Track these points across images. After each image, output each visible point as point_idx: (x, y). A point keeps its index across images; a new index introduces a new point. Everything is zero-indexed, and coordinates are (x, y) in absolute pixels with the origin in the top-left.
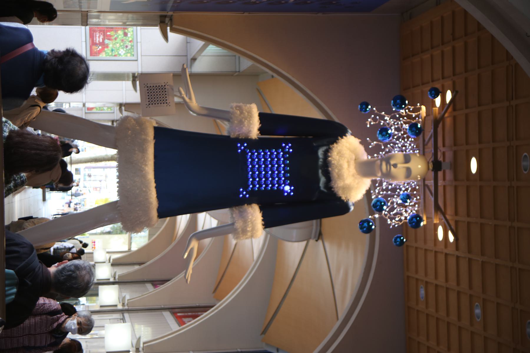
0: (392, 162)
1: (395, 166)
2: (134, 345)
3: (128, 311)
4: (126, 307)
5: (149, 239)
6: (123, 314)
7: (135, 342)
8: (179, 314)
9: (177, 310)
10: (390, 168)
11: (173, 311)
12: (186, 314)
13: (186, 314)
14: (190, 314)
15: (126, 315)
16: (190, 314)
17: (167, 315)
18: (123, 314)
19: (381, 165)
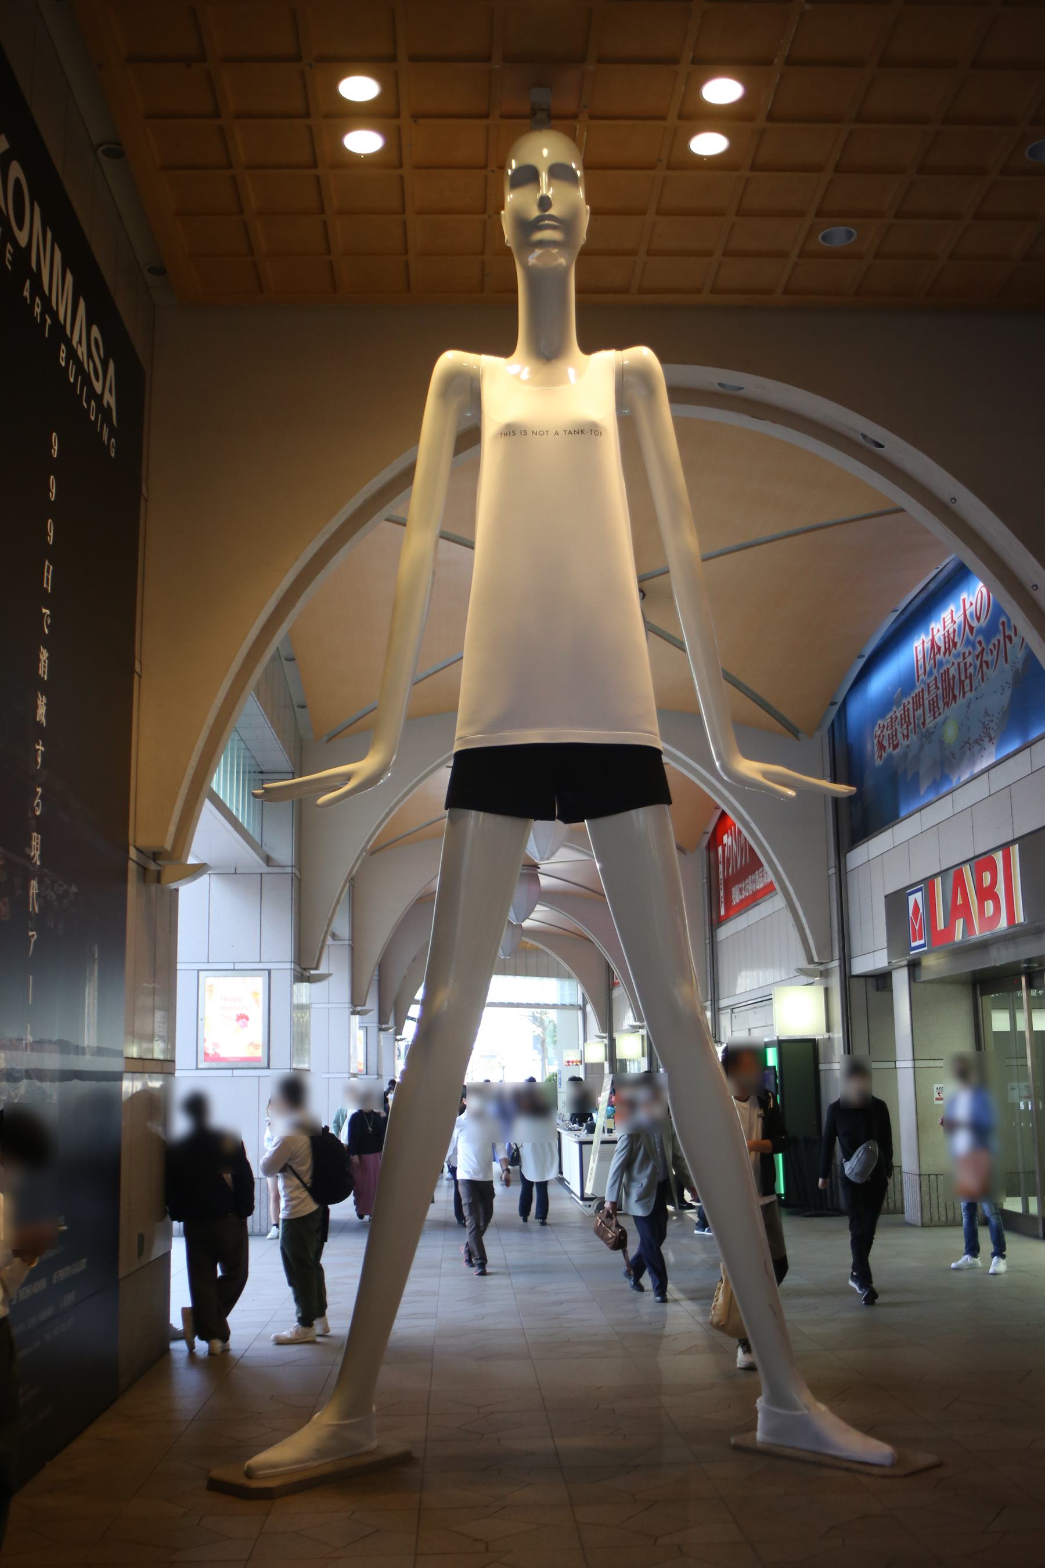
0: (535, 212)
1: (544, 203)
2: (811, 980)
3: (715, 1000)
4: (708, 1003)
5: (569, 977)
6: (719, 1009)
7: (805, 979)
8: (723, 913)
9: (714, 917)
10: (552, 218)
11: (715, 922)
12: (722, 900)
13: (722, 900)
14: (722, 894)
15: (723, 1003)
16: (722, 894)
17: (724, 932)
18: (719, 1009)
19: (541, 244)
